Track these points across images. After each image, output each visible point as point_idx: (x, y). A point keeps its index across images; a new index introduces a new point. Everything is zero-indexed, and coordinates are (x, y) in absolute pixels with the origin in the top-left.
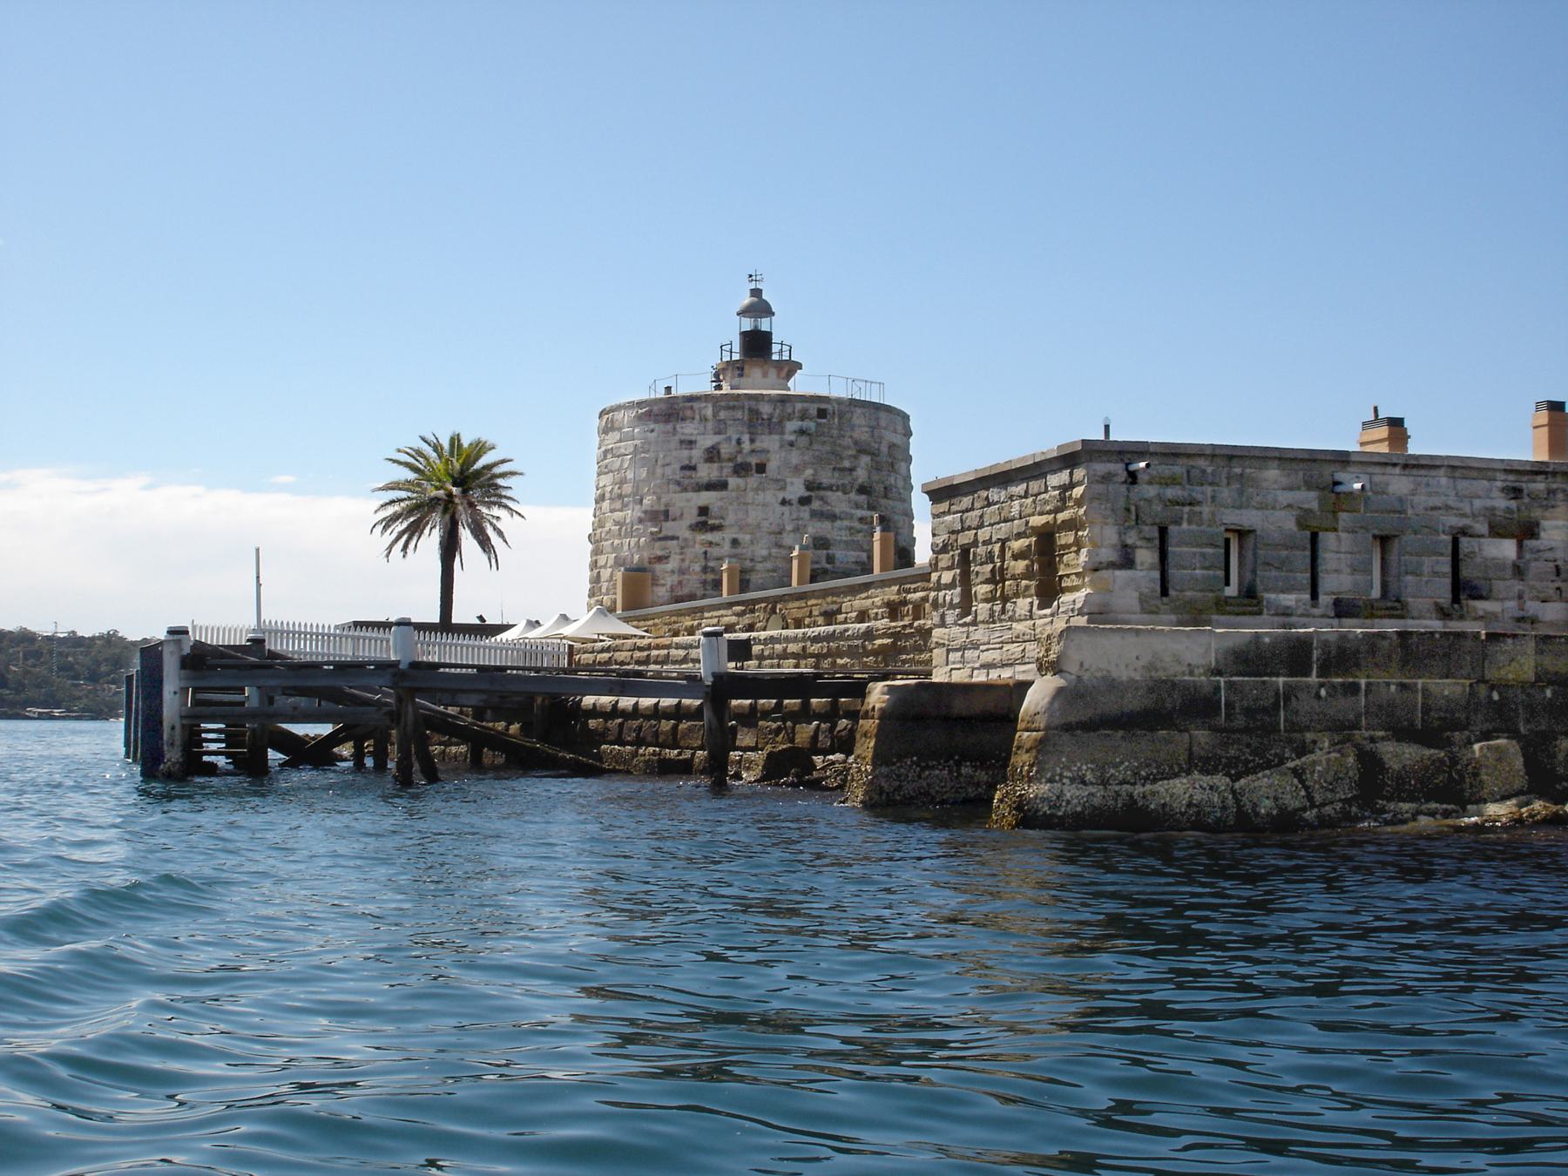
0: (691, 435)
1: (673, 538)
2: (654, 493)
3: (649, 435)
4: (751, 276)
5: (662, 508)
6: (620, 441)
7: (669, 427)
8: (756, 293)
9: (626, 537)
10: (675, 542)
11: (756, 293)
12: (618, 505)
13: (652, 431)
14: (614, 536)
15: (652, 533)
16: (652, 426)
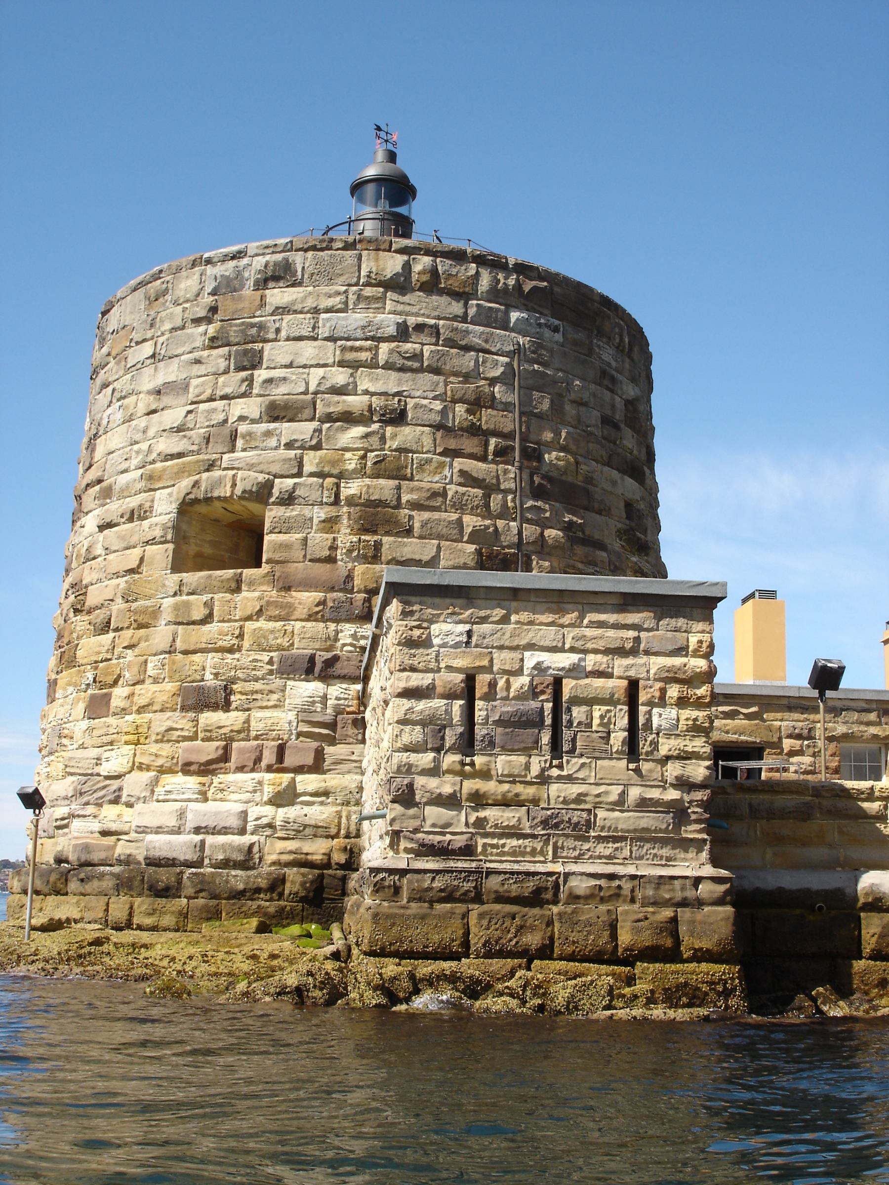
0: (609, 365)
1: (601, 546)
2: (563, 449)
3: (547, 333)
4: (379, 128)
5: (579, 481)
6: (464, 319)
7: (581, 336)
8: (392, 157)
9: (505, 513)
10: (604, 554)
11: (392, 157)
12: (470, 444)
13: (556, 330)
14: (460, 506)
15: (571, 524)
16: (557, 322)
